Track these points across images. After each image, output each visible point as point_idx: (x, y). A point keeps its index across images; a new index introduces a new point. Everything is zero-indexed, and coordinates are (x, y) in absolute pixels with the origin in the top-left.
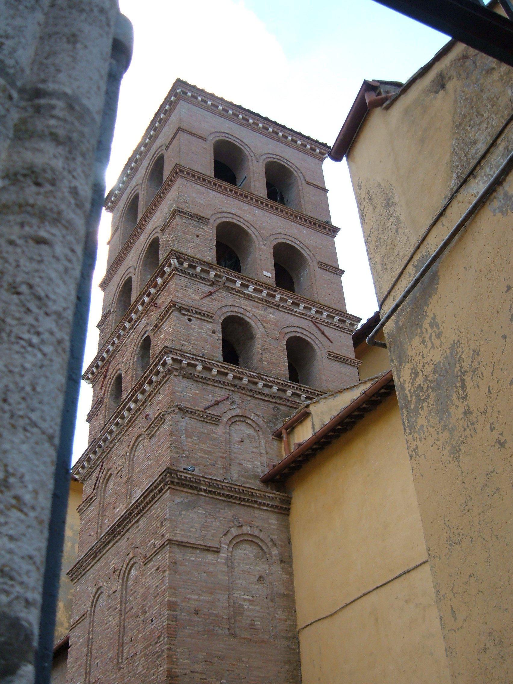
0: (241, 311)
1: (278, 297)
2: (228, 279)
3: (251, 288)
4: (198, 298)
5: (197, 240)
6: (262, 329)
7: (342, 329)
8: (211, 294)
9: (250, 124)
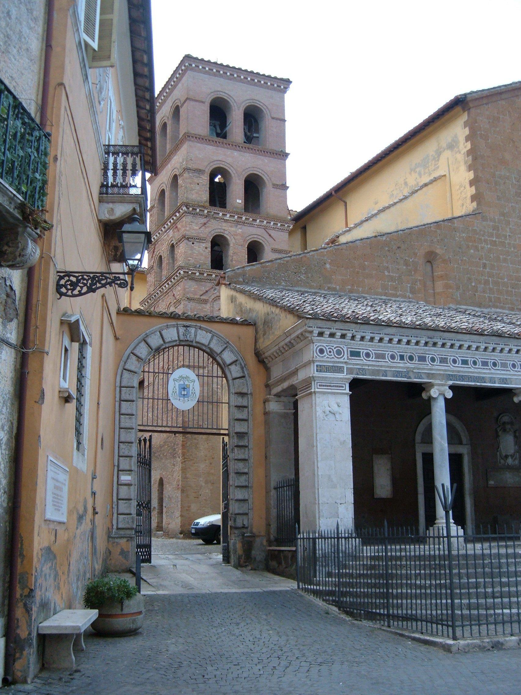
0: (222, 231)
1: (244, 218)
2: (215, 213)
5: (198, 187)
6: (233, 241)
7: (282, 230)
8: (205, 224)
9: (235, 78)
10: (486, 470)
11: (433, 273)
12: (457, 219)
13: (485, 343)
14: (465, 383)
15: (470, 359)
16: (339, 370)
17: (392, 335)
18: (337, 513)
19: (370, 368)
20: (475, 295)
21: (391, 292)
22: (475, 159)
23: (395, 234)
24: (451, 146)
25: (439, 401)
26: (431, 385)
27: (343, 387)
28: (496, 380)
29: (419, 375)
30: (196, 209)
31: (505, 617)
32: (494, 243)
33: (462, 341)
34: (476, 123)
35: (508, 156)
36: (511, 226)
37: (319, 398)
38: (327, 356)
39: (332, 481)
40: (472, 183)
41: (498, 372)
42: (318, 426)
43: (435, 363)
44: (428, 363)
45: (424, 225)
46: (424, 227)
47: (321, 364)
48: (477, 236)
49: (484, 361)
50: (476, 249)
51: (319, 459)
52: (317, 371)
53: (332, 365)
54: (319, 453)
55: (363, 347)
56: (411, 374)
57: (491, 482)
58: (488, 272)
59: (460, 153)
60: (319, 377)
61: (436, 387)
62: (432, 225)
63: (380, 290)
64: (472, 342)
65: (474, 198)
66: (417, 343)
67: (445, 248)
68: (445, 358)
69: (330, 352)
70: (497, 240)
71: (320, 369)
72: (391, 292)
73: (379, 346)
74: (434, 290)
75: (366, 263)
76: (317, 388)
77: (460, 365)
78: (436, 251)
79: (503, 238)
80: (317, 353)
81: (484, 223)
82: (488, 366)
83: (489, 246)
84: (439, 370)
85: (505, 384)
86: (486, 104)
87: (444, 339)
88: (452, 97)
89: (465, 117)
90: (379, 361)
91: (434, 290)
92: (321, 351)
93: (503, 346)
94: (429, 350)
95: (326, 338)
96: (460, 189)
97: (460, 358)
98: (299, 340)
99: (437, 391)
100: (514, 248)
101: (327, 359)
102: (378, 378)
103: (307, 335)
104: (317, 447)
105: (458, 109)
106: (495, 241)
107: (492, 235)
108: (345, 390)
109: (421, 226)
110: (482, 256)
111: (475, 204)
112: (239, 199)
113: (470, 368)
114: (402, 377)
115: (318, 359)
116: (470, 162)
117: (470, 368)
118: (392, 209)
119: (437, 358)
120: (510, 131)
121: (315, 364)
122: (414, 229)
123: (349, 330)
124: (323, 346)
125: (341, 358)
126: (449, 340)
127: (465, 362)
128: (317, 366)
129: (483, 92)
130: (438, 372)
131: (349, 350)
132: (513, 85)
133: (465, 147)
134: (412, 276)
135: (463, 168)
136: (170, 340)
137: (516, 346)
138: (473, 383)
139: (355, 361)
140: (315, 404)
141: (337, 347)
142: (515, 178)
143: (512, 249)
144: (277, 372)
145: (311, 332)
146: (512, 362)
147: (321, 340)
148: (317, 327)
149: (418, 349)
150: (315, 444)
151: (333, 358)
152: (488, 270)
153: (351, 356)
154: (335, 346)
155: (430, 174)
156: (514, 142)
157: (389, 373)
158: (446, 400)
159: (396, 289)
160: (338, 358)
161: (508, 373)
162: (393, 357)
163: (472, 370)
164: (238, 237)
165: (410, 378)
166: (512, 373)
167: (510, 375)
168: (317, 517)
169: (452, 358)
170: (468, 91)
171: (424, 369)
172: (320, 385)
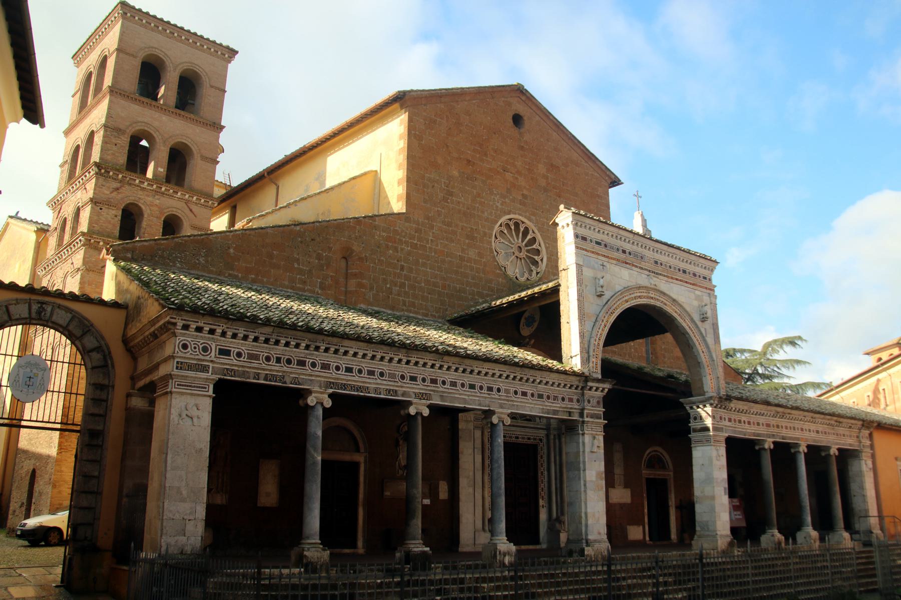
0: (137, 199)
2: (130, 178)
3: (146, 184)
4: (108, 192)
5: (115, 148)
6: (149, 211)
8: (117, 189)
11: (347, 270)
12: (379, 218)
15: (355, 367)
16: (205, 369)
18: (184, 530)
19: (240, 369)
20: (389, 297)
21: (298, 285)
23: (311, 225)
27: (206, 388)
30: (109, 172)
32: (414, 246)
33: (348, 347)
35: (440, 161)
36: (434, 231)
37: (176, 398)
38: (191, 352)
39: (181, 494)
41: (385, 382)
42: (171, 431)
43: (316, 369)
44: (307, 368)
45: (343, 219)
46: (342, 221)
47: (183, 361)
48: (398, 237)
49: (371, 371)
50: (396, 250)
52: (177, 368)
53: (195, 362)
55: (235, 346)
57: (387, 493)
58: (405, 275)
60: (178, 375)
61: (313, 395)
62: (351, 220)
63: (286, 283)
67: (363, 245)
69: (195, 348)
71: (180, 366)
72: (298, 285)
74: (346, 288)
75: (275, 252)
76: (175, 388)
77: (343, 373)
78: (353, 248)
79: (425, 242)
81: (407, 224)
82: (374, 376)
83: (409, 248)
90: (251, 362)
91: (346, 288)
92: (185, 346)
97: (344, 366)
99: (314, 399)
100: (435, 253)
101: (190, 355)
105: (397, 105)
106: (417, 244)
107: (413, 238)
108: (208, 391)
109: (340, 219)
110: (401, 257)
112: (161, 168)
113: (354, 376)
114: (276, 381)
115: (180, 354)
117: (354, 376)
119: (319, 362)
120: (445, 135)
121: (176, 360)
122: (332, 222)
124: (188, 341)
126: (334, 345)
127: (349, 370)
128: (178, 362)
131: (218, 347)
132: (454, 90)
134: (324, 271)
136: (18, 316)
138: (356, 393)
139: (224, 360)
140: (171, 405)
141: (204, 343)
142: (445, 183)
143: (433, 254)
144: (143, 364)
145: (175, 324)
146: (401, 373)
149: (298, 352)
151: (197, 355)
152: (405, 272)
154: (202, 341)
156: (447, 146)
158: (325, 409)
159: (305, 283)
160: (203, 355)
161: (396, 384)
162: (268, 359)
163: (356, 378)
164: (155, 208)
165: (285, 383)
166: (400, 384)
169: (336, 364)
170: (408, 89)
172: (178, 385)
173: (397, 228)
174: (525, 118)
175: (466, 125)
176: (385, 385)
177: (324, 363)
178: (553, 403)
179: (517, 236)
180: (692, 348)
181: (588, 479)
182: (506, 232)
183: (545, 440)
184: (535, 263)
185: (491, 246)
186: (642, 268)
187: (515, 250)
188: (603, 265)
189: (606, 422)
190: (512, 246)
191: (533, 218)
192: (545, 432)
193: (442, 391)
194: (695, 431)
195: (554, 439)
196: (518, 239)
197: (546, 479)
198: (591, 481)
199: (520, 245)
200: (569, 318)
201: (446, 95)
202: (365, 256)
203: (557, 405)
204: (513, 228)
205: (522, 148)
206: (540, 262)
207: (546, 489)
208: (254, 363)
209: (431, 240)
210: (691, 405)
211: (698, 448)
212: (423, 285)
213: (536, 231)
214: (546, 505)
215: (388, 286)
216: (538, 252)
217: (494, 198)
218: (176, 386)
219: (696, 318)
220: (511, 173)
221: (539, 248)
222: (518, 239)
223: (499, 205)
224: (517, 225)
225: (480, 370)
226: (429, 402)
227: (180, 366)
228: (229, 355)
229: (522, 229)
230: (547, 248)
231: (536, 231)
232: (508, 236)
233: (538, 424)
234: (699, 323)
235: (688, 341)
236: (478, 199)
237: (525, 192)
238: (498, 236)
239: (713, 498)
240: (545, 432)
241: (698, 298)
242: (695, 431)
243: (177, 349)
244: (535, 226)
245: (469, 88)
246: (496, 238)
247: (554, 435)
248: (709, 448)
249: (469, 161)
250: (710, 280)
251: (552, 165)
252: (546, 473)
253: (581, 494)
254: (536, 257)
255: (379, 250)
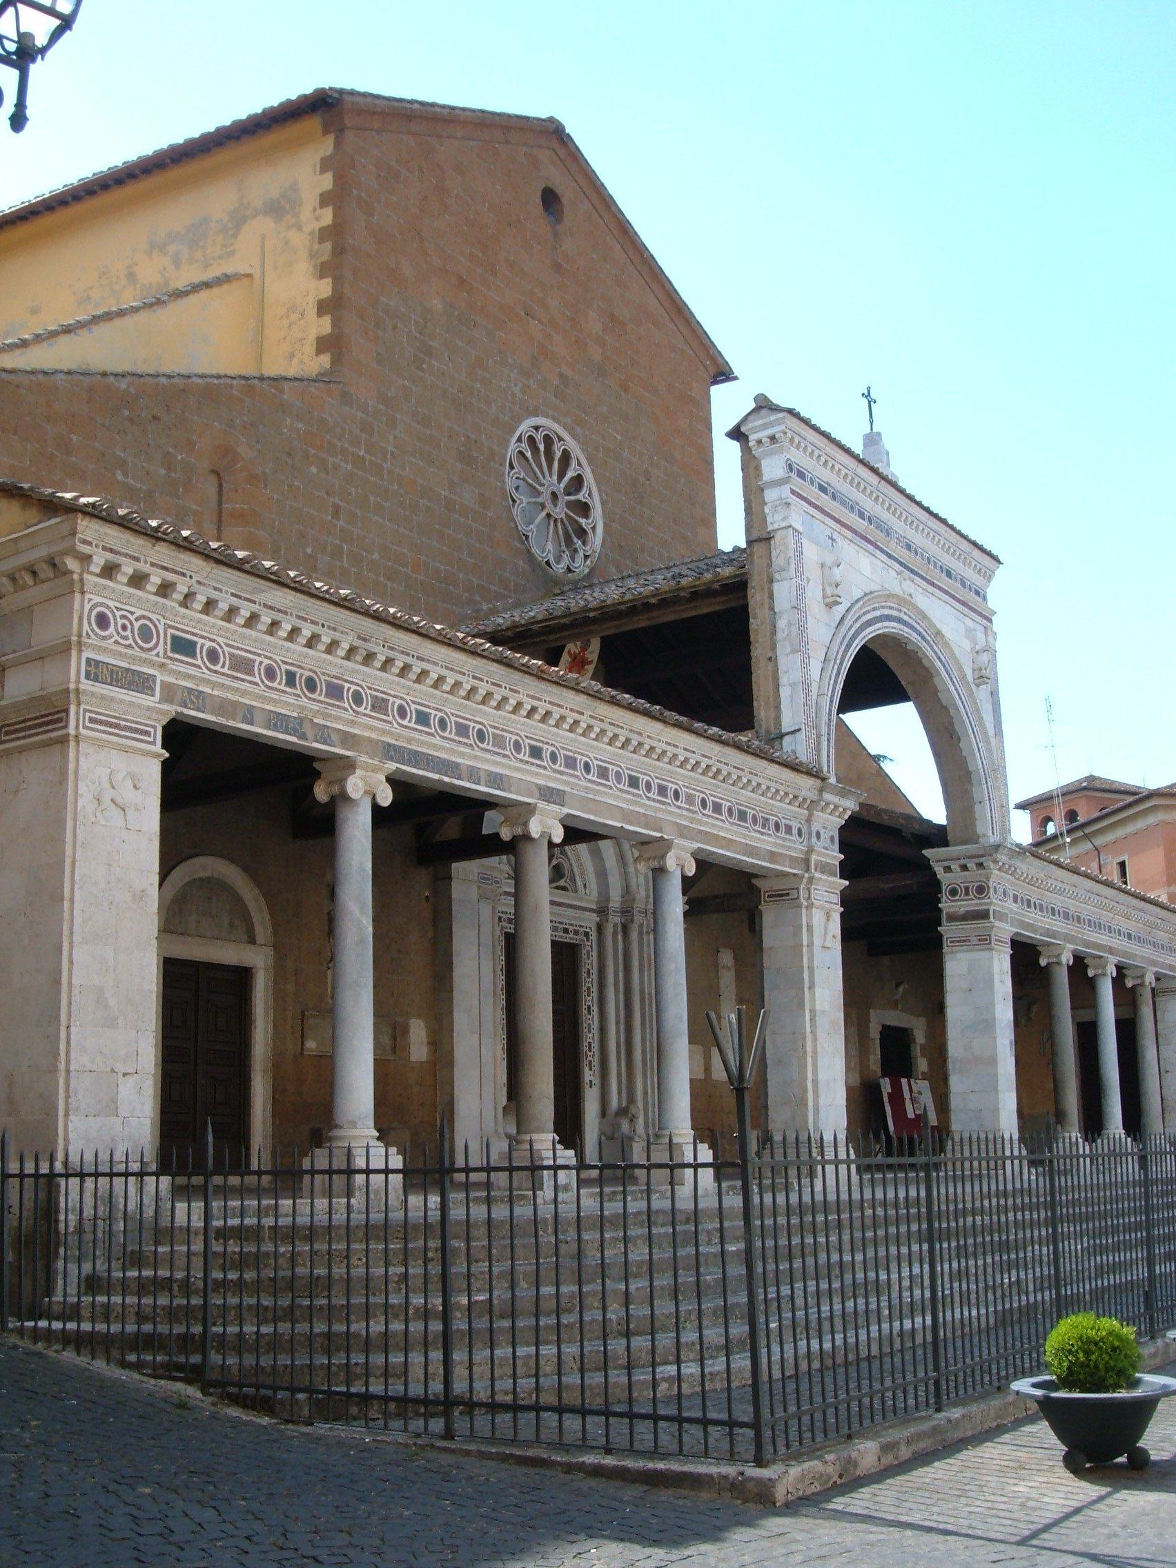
10: (303, 1012)
11: (220, 503)
12: (291, 384)
13: (474, 677)
14: (421, 772)
15: (433, 712)
16: (142, 683)
17: (280, 611)
18: (114, 1101)
19: (216, 693)
22: (339, 251)
23: (150, 380)
24: (276, 209)
25: (361, 810)
26: (348, 765)
28: (482, 774)
29: (324, 733)
31: (684, 1386)
33: (428, 661)
34: (353, 167)
37: (87, 755)
38: (116, 637)
39: (107, 1007)
40: (323, 307)
42: (80, 837)
43: (361, 709)
44: (346, 705)
45: (219, 377)
46: (215, 381)
47: (98, 658)
51: (77, 939)
52: (87, 677)
54: (78, 921)
56: (307, 728)
57: (311, 1044)
58: (342, 529)
59: (300, 228)
62: (235, 382)
64: (447, 668)
65: (323, 344)
66: (332, 647)
67: (259, 446)
68: (383, 699)
69: (124, 628)
70: (368, 457)
71: (96, 671)
73: (243, 637)
75: (74, 438)
76: (85, 727)
78: (239, 450)
80: (89, 623)
82: (468, 737)
84: (371, 728)
85: (498, 788)
86: (378, 132)
87: (392, 649)
88: (308, 90)
89: (327, 146)
90: (237, 679)
93: (507, 693)
94: (354, 671)
95: (120, 585)
96: (287, 316)
98: (28, 579)
99: (361, 784)
100: (399, 484)
102: (231, 723)
103: (72, 564)
104: (72, 900)
105: (313, 123)
106: (363, 458)
108: (153, 743)
109: (212, 376)
111: (325, 360)
113: (432, 735)
114: (287, 732)
115: (93, 640)
116: (325, 258)
117: (432, 735)
118: (129, 321)
119: (367, 695)
123: (183, 575)
124: (108, 607)
125: (151, 649)
126: (403, 652)
128: (88, 660)
129: (378, 102)
130: (367, 734)
131: (170, 631)
132: (438, 110)
133: (317, 219)
135: (303, 268)
137: (533, 697)
138: (436, 777)
141: (144, 617)
142: (416, 323)
143: (396, 487)
145: (86, 559)
147: (105, 587)
148: (104, 548)
150: (67, 894)
151: (130, 646)
152: (341, 523)
153: (174, 650)
154: (139, 613)
155: (206, 266)
157: (258, 717)
158: (376, 809)
160: (142, 648)
165: (303, 736)
167: (510, 767)
168: (61, 1112)
169: (398, 702)
170: (348, 86)
171: (338, 718)
172: (91, 720)
173: (326, 416)
174: (565, 201)
175: (457, 196)
176: (487, 760)
177: (376, 697)
178: (762, 834)
179: (550, 466)
180: (959, 739)
181: (818, 1007)
182: (529, 455)
183: (594, 937)
184: (582, 533)
185: (504, 483)
186: (890, 556)
187: (545, 498)
188: (833, 540)
189: (847, 883)
190: (541, 489)
191: (578, 430)
192: (595, 918)
193: (587, 788)
194: (953, 918)
195: (615, 934)
196: (551, 475)
197: (595, 1026)
198: (823, 1012)
199: (555, 489)
200: (773, 647)
201: (421, 117)
202: (264, 473)
203: (768, 842)
204: (542, 447)
205: (558, 267)
206: (590, 532)
207: (596, 1045)
208: (243, 680)
209: (392, 453)
210: (946, 864)
211: (959, 955)
212: (376, 556)
213: (584, 462)
214: (597, 1081)
215: (309, 550)
216: (584, 509)
217: (509, 376)
218: (88, 724)
219: (970, 678)
220: (539, 321)
221: (589, 501)
222: (551, 475)
223: (516, 390)
224: (548, 440)
225: (655, 744)
226: (566, 810)
227: (96, 671)
228: (193, 655)
229: (558, 454)
230: (603, 503)
231: (584, 462)
232: (533, 465)
233: (580, 899)
234: (973, 687)
235: (952, 723)
236: (480, 372)
237: (565, 370)
238: (515, 464)
239: (992, 1061)
240: (595, 918)
241: (969, 634)
242: (953, 918)
243: (86, 627)
244: (583, 450)
245: (464, 109)
246: (512, 467)
247: (615, 926)
248: (985, 954)
249: (462, 281)
250: (985, 598)
251: (613, 318)
252: (595, 1009)
253: (804, 1038)
254: (583, 521)
255: (290, 462)
